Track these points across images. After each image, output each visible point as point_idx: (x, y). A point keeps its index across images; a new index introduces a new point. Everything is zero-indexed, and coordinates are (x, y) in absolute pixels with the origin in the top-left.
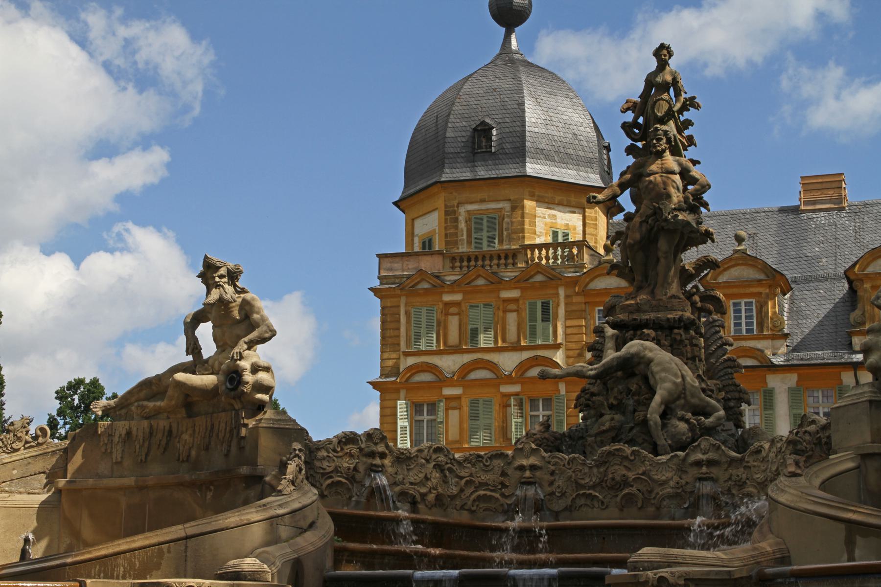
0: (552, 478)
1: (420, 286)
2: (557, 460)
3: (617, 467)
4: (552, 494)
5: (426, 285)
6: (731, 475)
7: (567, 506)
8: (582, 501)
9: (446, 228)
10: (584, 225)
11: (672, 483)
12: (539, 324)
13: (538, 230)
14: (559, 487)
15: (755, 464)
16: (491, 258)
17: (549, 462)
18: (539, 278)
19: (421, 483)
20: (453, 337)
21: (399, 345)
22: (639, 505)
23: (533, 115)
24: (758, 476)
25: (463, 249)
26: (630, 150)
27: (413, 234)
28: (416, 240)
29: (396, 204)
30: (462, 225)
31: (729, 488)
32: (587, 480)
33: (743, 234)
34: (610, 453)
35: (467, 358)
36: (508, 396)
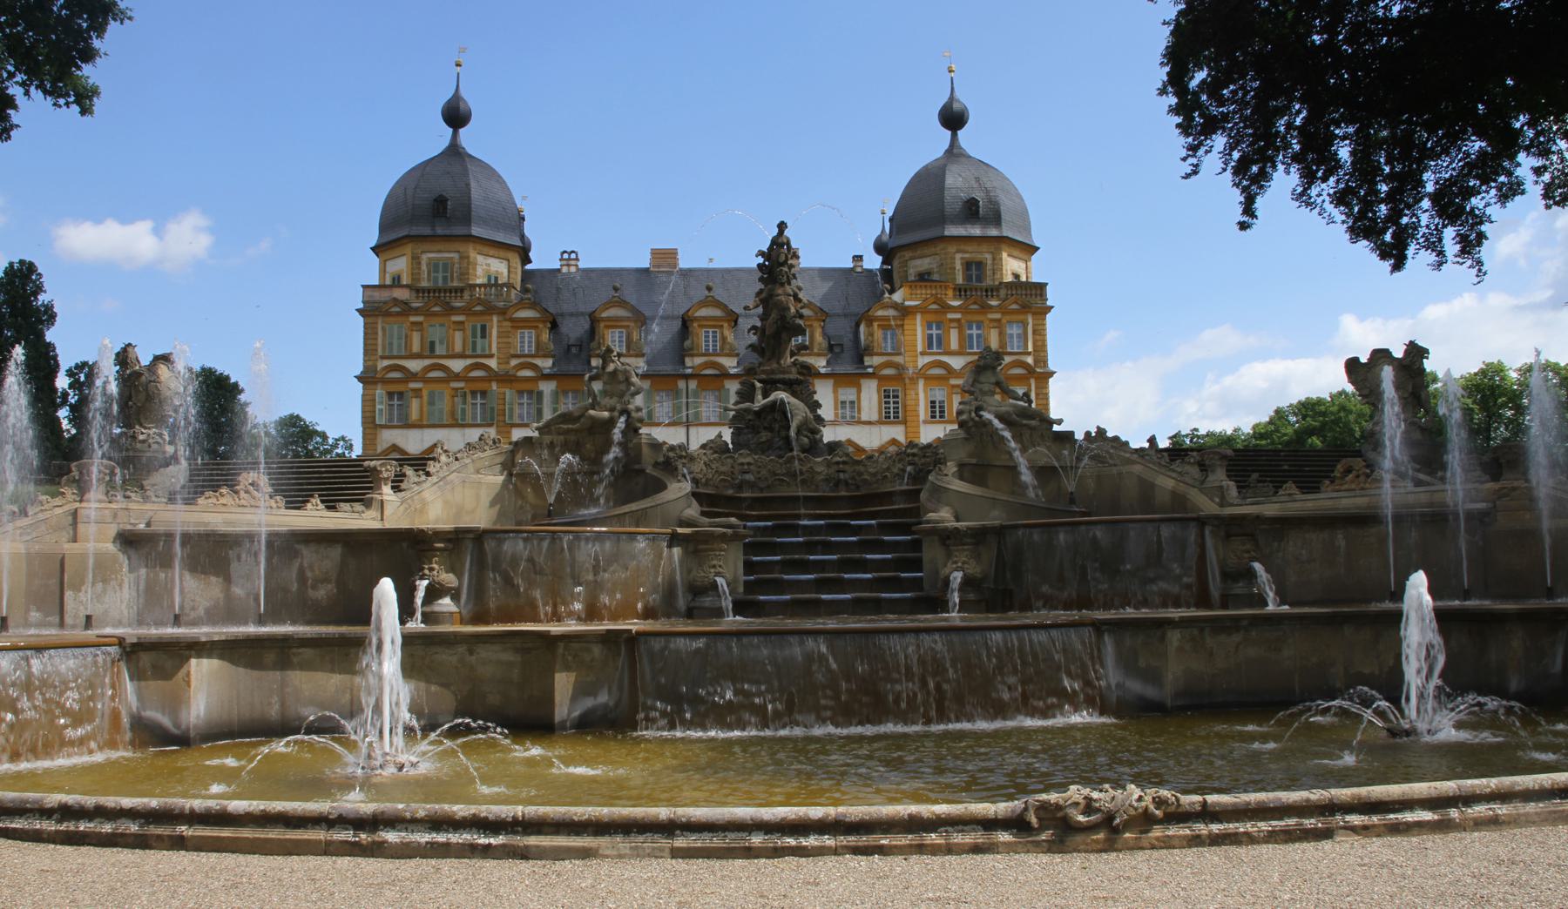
1: (393, 310)
5: (398, 309)
8: (777, 483)
9: (412, 269)
10: (509, 272)
12: (479, 340)
13: (478, 273)
16: (445, 291)
18: (479, 308)
19: (700, 473)
20: (416, 348)
21: (377, 350)
23: (476, 194)
25: (424, 284)
26: (761, 280)
27: (385, 271)
28: (387, 275)
29: (372, 249)
30: (424, 267)
33: (618, 285)
35: (427, 362)
36: (456, 389)
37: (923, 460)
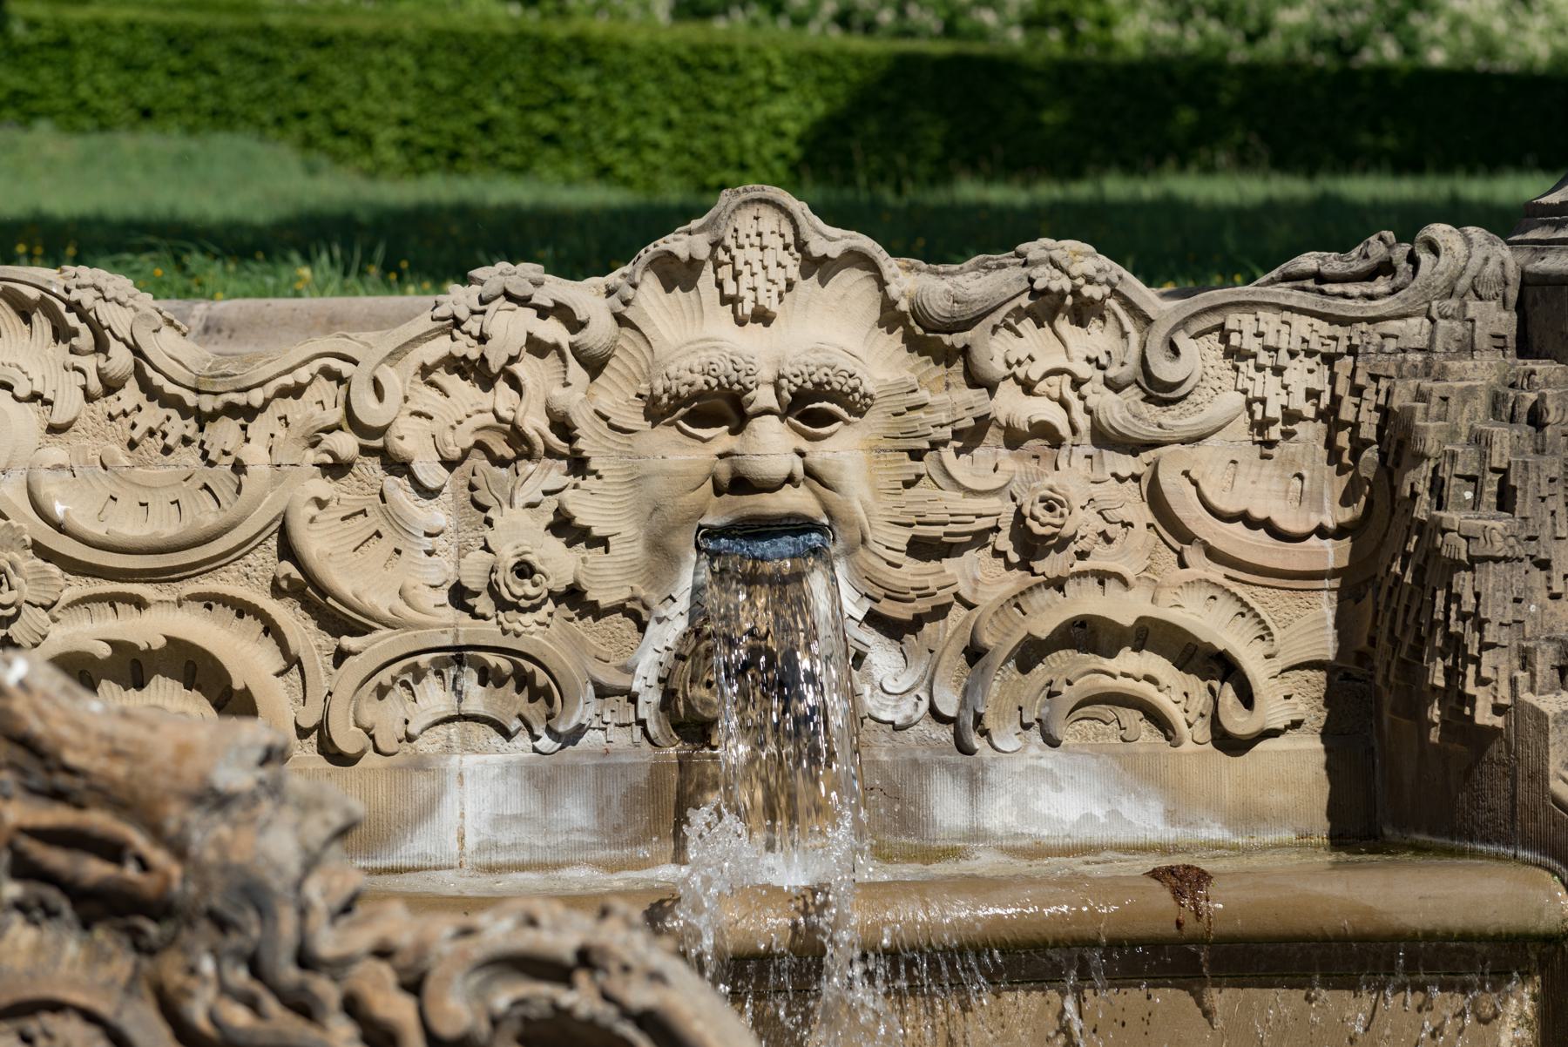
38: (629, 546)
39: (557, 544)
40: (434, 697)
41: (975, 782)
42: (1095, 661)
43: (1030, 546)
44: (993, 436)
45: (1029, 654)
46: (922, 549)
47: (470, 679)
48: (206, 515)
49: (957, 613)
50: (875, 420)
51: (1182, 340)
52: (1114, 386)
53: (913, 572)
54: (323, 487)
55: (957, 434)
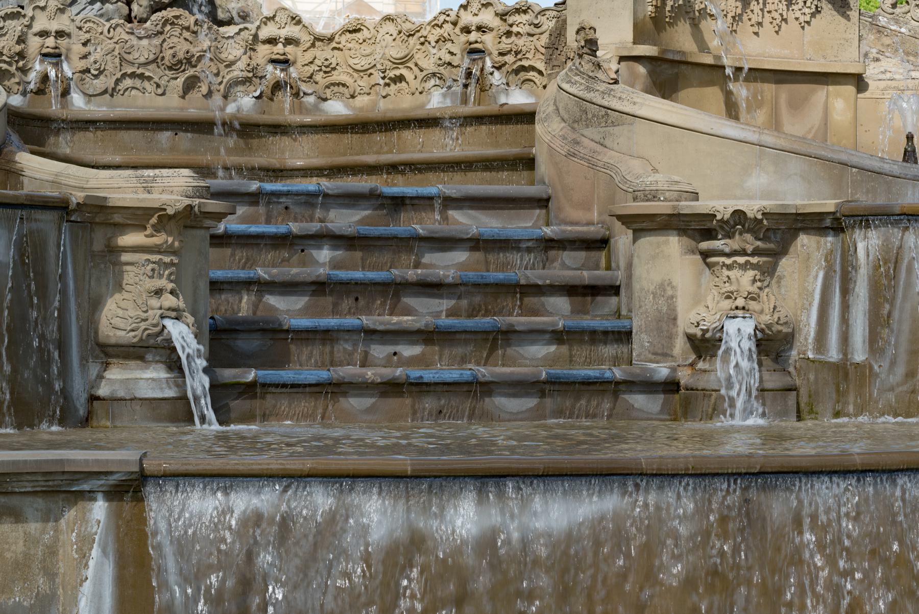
0: (85, 50)
2: (91, 25)
3: (175, 40)
4: (88, 71)
6: (315, 58)
7: (107, 89)
8: (128, 82)
11: (241, 65)
14: (95, 62)
15: (349, 45)
17: (80, 28)
22: (204, 89)
24: (356, 61)
31: (312, 74)
32: (136, 55)
34: (166, 22)
37: (506, 44)
38: (459, 56)
39: (449, 55)
40: (432, 82)
41: (507, 95)
42: (526, 74)
43: (517, 53)
44: (513, 35)
45: (517, 72)
46: (501, 54)
47: (437, 79)
48: (407, 52)
49: (507, 66)
50: (495, 32)
51: (539, 16)
52: (530, 25)
53: (500, 58)
54: (419, 47)
55: (504, 34)
